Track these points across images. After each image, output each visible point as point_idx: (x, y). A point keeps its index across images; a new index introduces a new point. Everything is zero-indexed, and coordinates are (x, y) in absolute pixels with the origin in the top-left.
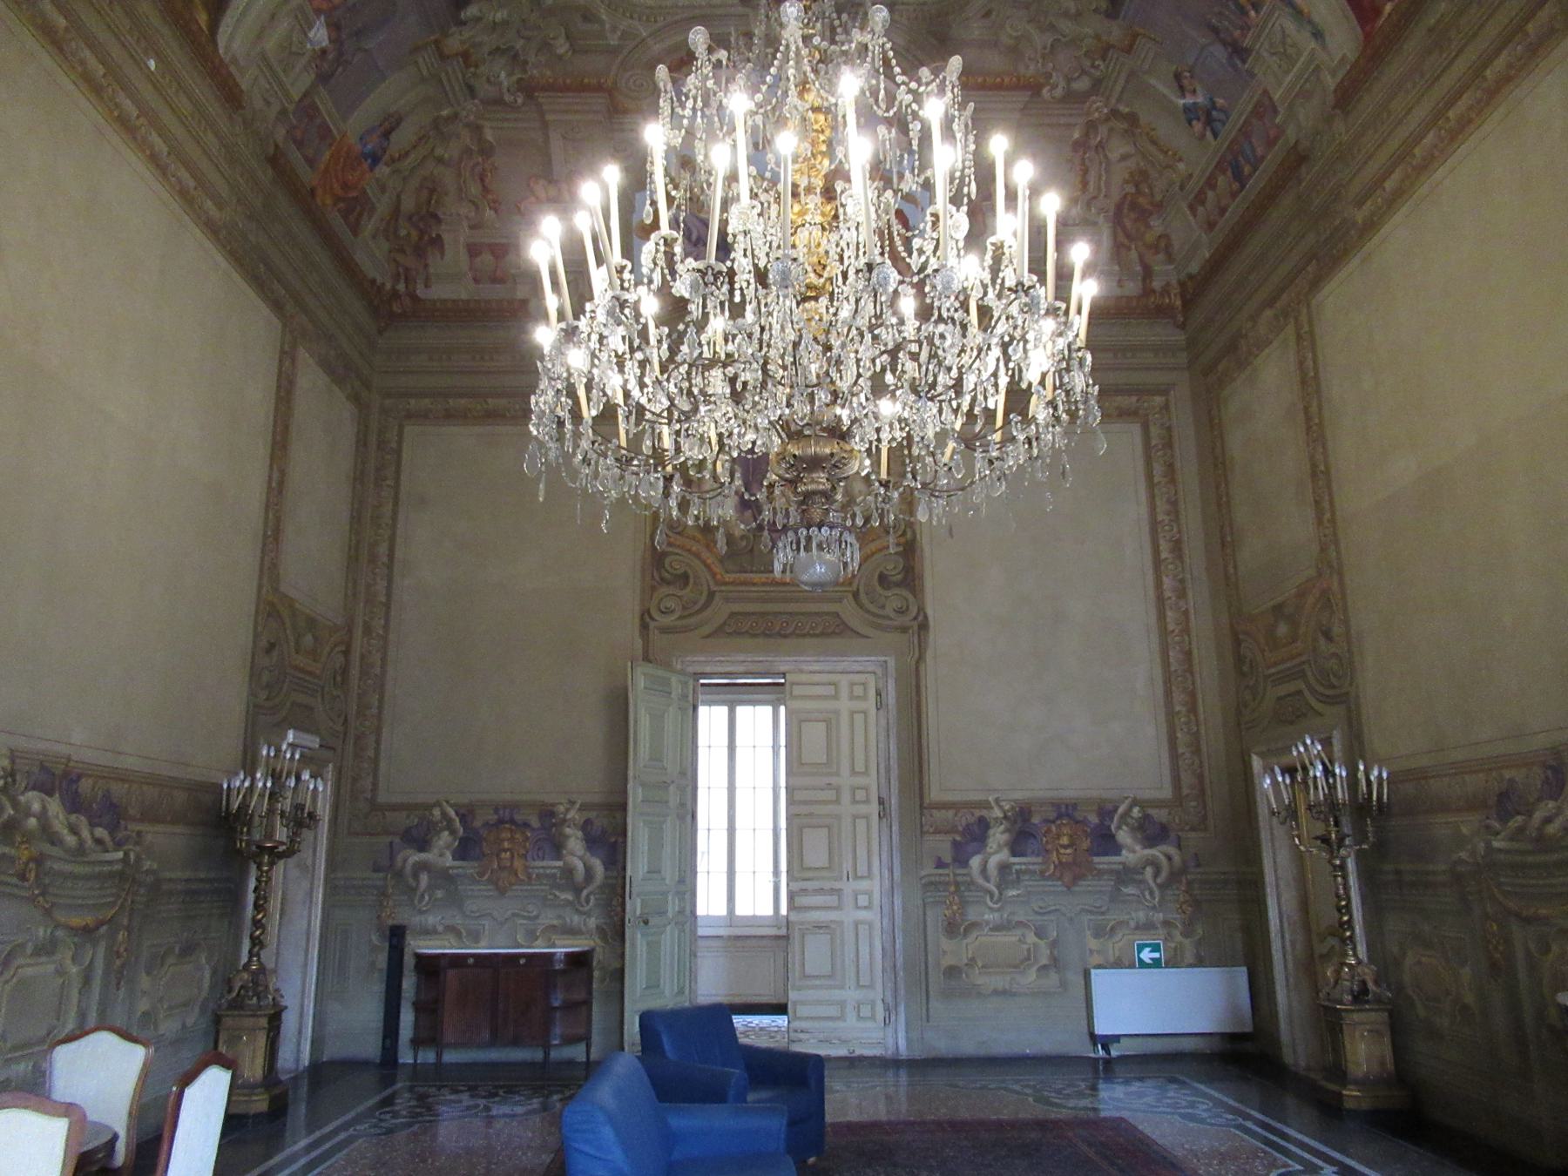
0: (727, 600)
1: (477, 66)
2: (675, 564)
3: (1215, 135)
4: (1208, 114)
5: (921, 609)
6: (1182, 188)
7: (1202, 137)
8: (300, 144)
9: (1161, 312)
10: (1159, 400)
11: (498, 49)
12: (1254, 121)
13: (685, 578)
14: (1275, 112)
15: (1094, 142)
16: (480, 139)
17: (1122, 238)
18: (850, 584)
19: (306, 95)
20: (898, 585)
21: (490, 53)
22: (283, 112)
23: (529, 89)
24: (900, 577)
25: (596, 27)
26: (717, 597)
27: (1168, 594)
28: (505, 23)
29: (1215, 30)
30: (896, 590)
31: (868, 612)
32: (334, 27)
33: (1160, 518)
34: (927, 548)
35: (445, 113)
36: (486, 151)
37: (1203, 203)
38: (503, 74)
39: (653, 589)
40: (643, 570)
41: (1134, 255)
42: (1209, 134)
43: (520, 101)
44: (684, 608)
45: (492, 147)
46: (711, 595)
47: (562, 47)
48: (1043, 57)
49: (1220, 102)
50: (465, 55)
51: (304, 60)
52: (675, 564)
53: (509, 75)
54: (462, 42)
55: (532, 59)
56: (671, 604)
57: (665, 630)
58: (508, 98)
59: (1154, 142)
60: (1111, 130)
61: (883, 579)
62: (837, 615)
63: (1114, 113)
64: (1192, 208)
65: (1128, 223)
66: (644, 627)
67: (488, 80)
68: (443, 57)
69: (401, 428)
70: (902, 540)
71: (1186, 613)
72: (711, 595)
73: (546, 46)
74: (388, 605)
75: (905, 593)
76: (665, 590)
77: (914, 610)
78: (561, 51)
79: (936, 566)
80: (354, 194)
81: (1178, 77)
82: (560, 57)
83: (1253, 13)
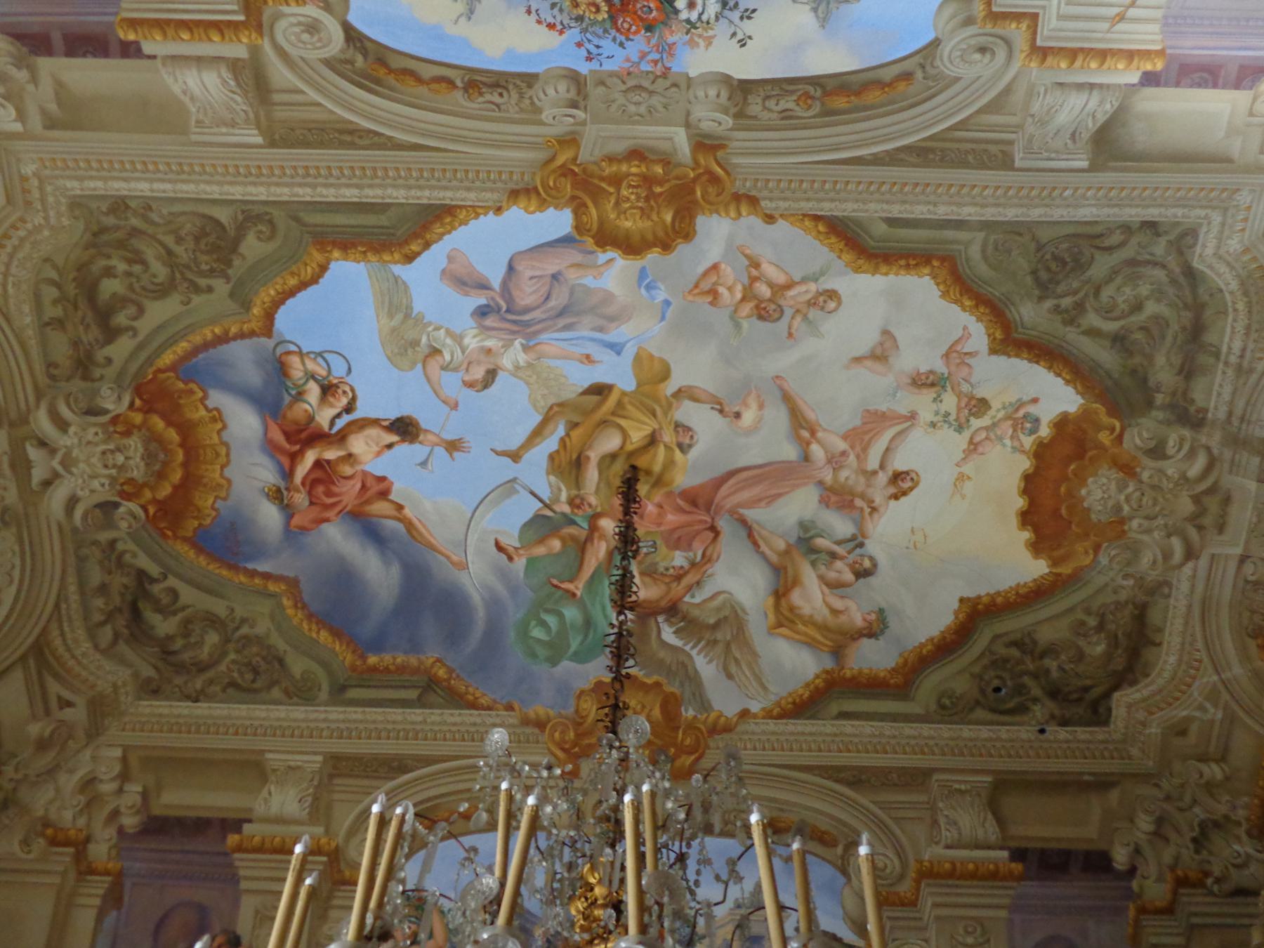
1: (1207, 874)
21: (1197, 852)
25: (1194, 728)
38: (1237, 847)
47: (1214, 771)
54: (1160, 879)
68: (1169, 910)
73: (1210, 787)
78: (1219, 775)
82: (1227, 778)
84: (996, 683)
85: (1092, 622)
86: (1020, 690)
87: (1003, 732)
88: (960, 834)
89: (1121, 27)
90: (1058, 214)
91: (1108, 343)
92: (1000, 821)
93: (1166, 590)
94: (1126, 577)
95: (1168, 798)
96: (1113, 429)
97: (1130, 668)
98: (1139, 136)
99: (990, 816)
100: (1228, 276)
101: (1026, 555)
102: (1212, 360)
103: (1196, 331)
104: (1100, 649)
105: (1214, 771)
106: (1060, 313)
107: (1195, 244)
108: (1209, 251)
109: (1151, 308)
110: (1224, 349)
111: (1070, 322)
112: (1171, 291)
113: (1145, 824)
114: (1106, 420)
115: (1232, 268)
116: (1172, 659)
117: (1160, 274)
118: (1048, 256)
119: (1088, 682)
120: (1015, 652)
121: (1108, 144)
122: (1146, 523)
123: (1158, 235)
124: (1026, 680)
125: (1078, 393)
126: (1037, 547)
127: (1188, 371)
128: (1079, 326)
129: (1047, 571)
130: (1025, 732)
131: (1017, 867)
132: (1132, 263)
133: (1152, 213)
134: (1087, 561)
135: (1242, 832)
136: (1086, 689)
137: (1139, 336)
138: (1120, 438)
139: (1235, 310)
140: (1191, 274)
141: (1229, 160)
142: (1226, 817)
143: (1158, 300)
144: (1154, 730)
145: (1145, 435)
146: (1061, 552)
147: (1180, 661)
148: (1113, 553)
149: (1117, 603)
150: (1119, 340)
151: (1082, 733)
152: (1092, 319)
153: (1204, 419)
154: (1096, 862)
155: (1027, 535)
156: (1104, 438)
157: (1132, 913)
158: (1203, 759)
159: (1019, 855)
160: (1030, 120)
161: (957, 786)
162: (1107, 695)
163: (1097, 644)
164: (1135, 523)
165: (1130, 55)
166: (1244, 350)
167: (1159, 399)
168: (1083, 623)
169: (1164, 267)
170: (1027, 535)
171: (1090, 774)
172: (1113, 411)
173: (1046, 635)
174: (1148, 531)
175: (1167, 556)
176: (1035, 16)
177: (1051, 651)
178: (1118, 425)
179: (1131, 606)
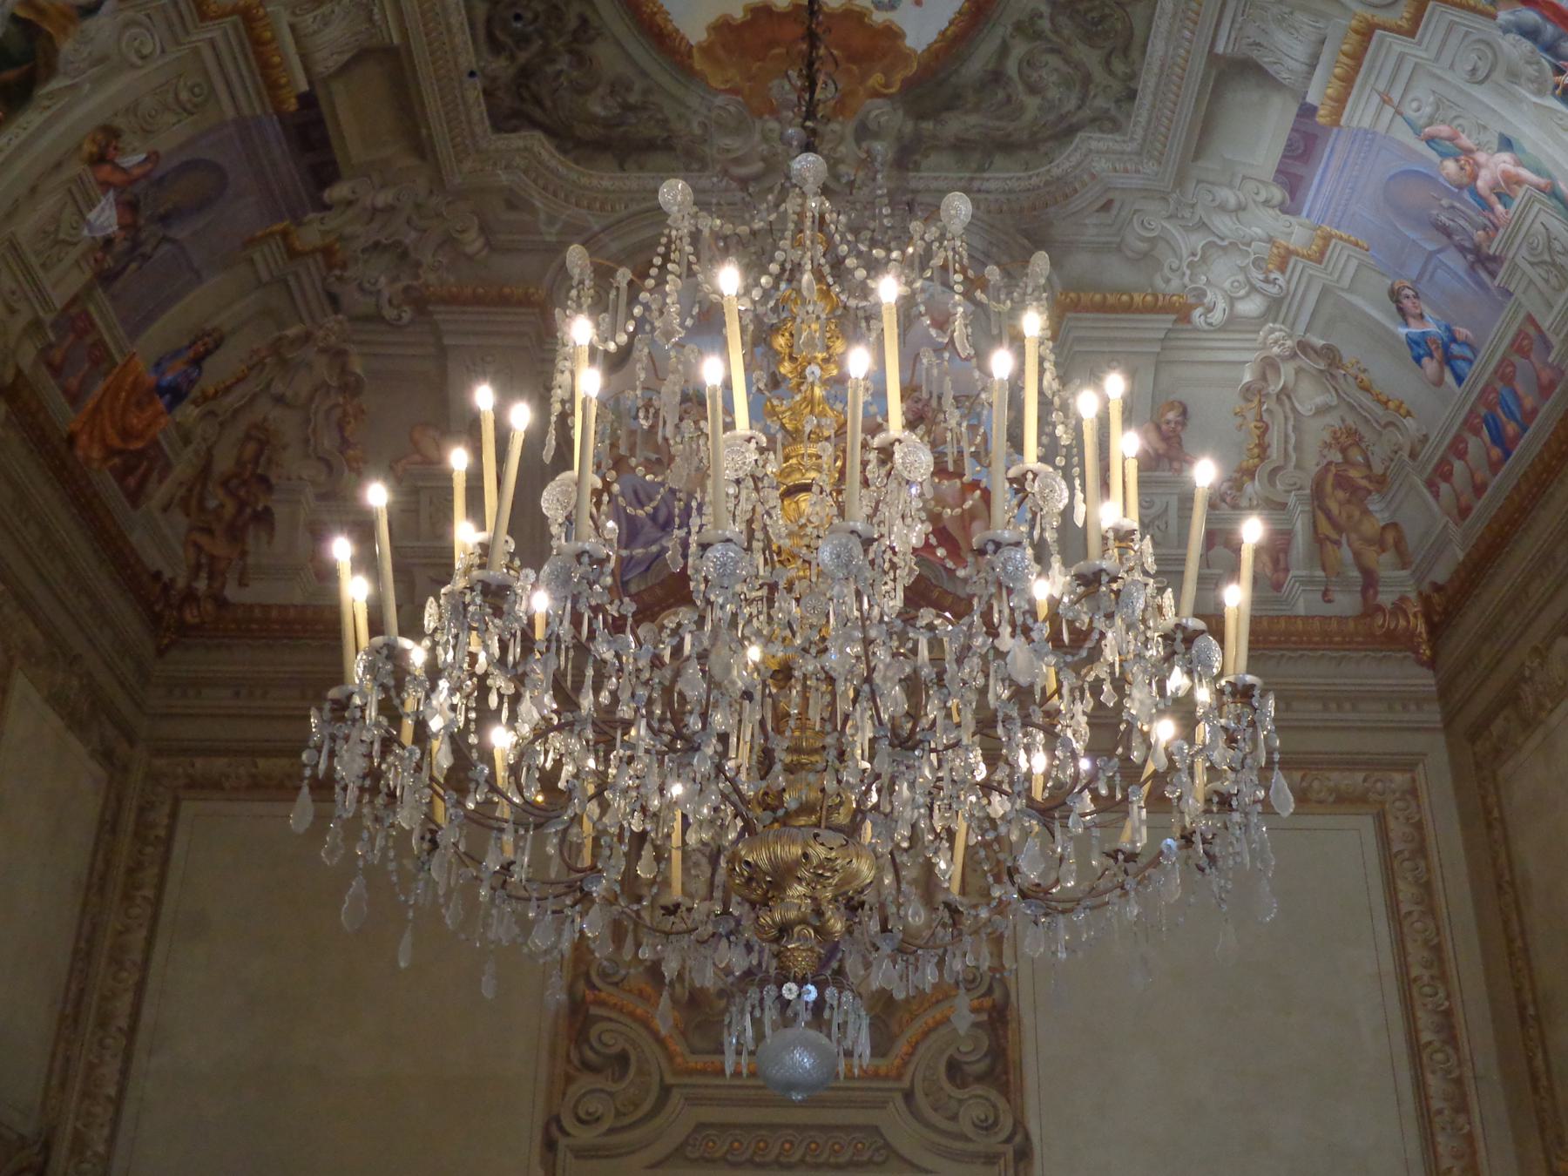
0: (693, 1101)
1: (344, 266)
2: (608, 1036)
3: (1459, 379)
4: (1446, 348)
5: (1019, 1125)
6: (1413, 455)
7: (1439, 382)
8: (56, 370)
9: (1391, 639)
10: (1399, 779)
11: (376, 245)
12: (1516, 359)
13: (622, 1060)
14: (1548, 346)
15: (1274, 388)
16: (344, 370)
17: (1325, 527)
18: (899, 1077)
19: (74, 300)
20: (980, 1079)
21: (364, 251)
22: (36, 325)
23: (420, 303)
24: (981, 1067)
26: (676, 1097)
27: (1436, 1104)
28: (390, 209)
29: (1446, 231)
30: (979, 1090)
31: (928, 1125)
32: (129, 207)
33: (1415, 971)
34: (1027, 1021)
35: (292, 332)
36: (351, 387)
37: (1447, 477)
38: (383, 280)
39: (569, 1080)
40: (553, 1054)
41: (1346, 553)
42: (1449, 378)
43: (406, 317)
44: (618, 1114)
45: (359, 380)
46: (666, 1090)
47: (473, 243)
48: (1191, 265)
49: (1462, 332)
50: (327, 252)
51: (75, 253)
52: (608, 1036)
53: (394, 280)
54: (325, 233)
55: (427, 258)
56: (594, 1105)
57: (583, 1153)
58: (389, 313)
59: (1366, 389)
60: (1299, 371)
61: (954, 1068)
62: (875, 1130)
63: (1304, 347)
64: (1431, 484)
65: (1334, 507)
66: (550, 1145)
67: (361, 288)
68: (293, 254)
69: (176, 802)
70: (987, 1002)
71: (1470, 1138)
72: (666, 1090)
73: (449, 241)
74: (118, 1102)
75: (994, 1095)
76: (586, 1081)
77: (1007, 1123)
78: (470, 249)
79: (1041, 1045)
80: (139, 445)
81: (1395, 295)
82: (470, 258)
83: (1499, 208)
84: (529, 15)
85: (633, 99)
86: (523, 40)
87: (463, 38)
88: (315, 32)
89: (1376, 99)
90: (1162, 24)
91: (990, 67)
92: (345, 68)
93: (695, 166)
94: (704, 125)
95: (418, 206)
96: (887, 86)
97: (580, 143)
98: (1242, 96)
99: (346, 57)
100: (1067, 165)
101: (711, 16)
102: (974, 166)
103: (1007, 146)
104: (598, 110)
105: (473, 243)
106: (1031, 18)
107: (1102, 131)
108: (1094, 145)
109: (1032, 103)
110: (986, 175)
111: (1019, 27)
112: (1052, 117)
113: (383, 198)
114: (898, 78)
115: (1075, 167)
116: (606, 183)
117: (1072, 104)
118: (1107, 11)
119: (548, 104)
120: (573, 23)
121: (1239, 71)
122: (776, 135)
123: (1117, 101)
124: (537, 44)
125: (930, 46)
126: (723, 28)
127: (961, 147)
128: (1013, 37)
129: (693, 42)
130: (467, 59)
131: (292, 105)
132: (1087, 79)
133: (1145, 99)
134: (716, 82)
135: (405, 282)
136: (538, 102)
137: (1001, 95)
138: (876, 94)
139: (1030, 177)
140: (1072, 131)
141: (1196, 158)
142: (418, 264)
143: (1040, 108)
144: (504, 178)
145: (883, 119)
146: (720, 53)
147: (606, 191)
148: (732, 109)
149: (666, 121)
150: (996, 77)
151: (479, 111)
152: (1019, 49)
153: (908, 170)
154: (324, 172)
155: (739, 15)
156: (876, 79)
157: (278, 227)
158: (483, 230)
159: (308, 101)
160: (1288, 10)
161: (376, 10)
162: (535, 124)
163: (605, 107)
164: (773, 125)
165: (1341, 101)
166: (988, 192)
167: (928, 126)
168: (629, 89)
169: (1079, 108)
170: (739, 15)
171: (430, 136)
172: (908, 84)
173: (602, 52)
174: (765, 139)
175: (738, 161)
176: (1411, 33)
177: (581, 60)
178: (893, 90)
179: (665, 135)
